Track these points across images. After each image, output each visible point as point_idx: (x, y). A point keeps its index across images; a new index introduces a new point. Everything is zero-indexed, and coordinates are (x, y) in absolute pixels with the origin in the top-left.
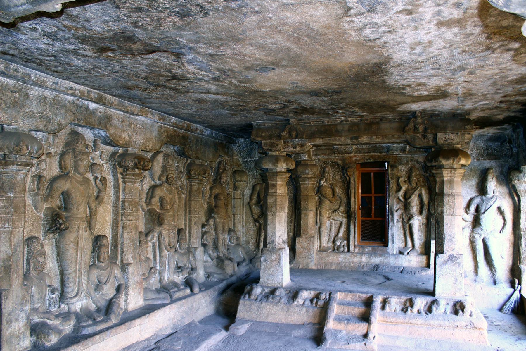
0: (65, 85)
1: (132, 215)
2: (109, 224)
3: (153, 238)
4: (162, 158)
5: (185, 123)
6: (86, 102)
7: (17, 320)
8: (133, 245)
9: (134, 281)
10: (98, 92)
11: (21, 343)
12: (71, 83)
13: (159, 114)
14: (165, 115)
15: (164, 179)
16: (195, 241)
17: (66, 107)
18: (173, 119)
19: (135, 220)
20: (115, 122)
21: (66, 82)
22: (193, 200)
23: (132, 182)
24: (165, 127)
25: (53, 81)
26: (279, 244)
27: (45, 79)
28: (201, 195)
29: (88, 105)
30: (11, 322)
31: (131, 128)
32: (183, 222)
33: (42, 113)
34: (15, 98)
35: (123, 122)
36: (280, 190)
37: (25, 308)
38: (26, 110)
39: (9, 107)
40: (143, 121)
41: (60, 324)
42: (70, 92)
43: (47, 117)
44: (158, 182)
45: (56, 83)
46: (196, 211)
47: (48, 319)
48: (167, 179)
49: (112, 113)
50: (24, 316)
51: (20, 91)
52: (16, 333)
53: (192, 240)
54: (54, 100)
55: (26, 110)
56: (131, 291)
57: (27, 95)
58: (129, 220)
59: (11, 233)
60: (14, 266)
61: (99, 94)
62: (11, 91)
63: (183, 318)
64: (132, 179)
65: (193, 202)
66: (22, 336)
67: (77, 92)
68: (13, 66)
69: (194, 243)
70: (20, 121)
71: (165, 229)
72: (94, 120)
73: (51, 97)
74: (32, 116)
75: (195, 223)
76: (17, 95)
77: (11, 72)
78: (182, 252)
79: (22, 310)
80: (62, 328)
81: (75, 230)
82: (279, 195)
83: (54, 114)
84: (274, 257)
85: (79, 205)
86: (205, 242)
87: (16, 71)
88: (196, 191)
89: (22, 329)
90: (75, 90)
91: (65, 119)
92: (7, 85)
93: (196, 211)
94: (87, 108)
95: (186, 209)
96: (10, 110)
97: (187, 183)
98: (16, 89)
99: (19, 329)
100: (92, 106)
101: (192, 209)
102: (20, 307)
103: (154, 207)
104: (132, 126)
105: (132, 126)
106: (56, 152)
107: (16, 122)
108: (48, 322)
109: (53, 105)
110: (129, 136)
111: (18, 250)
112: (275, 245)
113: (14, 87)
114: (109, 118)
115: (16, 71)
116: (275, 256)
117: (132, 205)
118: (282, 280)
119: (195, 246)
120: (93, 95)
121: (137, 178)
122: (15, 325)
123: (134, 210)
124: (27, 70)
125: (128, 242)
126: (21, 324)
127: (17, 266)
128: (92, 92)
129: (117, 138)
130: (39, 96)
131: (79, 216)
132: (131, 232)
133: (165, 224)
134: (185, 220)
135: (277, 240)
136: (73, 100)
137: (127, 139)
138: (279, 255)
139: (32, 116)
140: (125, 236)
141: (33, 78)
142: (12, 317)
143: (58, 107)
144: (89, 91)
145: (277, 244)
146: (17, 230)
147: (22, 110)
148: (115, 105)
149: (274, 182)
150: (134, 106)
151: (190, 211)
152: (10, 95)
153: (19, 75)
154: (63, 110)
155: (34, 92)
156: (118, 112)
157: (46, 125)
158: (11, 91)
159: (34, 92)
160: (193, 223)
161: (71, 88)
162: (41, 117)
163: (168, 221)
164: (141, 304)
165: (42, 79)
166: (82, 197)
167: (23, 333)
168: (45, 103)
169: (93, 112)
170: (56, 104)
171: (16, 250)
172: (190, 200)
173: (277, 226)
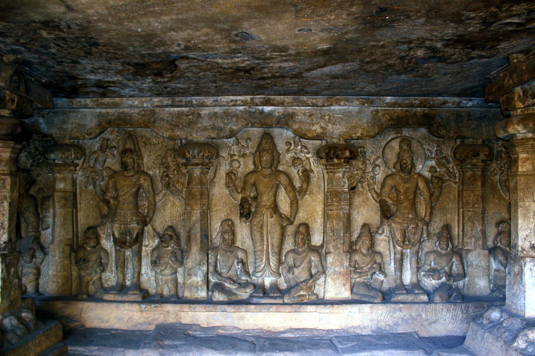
0: (225, 100)
1: (333, 205)
2: (320, 213)
3: (383, 232)
4: (398, 144)
5: (415, 99)
6: (260, 108)
7: (195, 275)
8: (334, 234)
9: (335, 271)
10: (263, 96)
11: (199, 293)
12: (231, 97)
13: (361, 98)
14: (370, 97)
15: (398, 167)
16: (468, 241)
17: (237, 116)
18: (388, 99)
19: (337, 210)
20: (299, 117)
21: (226, 97)
22: (466, 190)
23: (331, 172)
24: (384, 110)
25: (212, 100)
26: (523, 250)
27: (205, 101)
28: (479, 184)
29: (263, 109)
30: (191, 275)
31: (325, 119)
32: (456, 218)
33: (214, 125)
34: (189, 119)
35: (310, 116)
36: (522, 166)
37: (203, 269)
38: (199, 125)
39: (185, 126)
40: (343, 110)
41: (236, 289)
42: (231, 104)
43: (219, 127)
44: (394, 170)
45: (217, 100)
46: (469, 204)
47: (225, 281)
48: (401, 166)
49: (294, 111)
50: (202, 274)
51: (193, 114)
52: (195, 284)
53: (465, 240)
54: (224, 113)
55: (199, 125)
56: (329, 280)
57: (199, 115)
58: (330, 210)
59: (191, 213)
60: (193, 237)
61: (264, 98)
62: (187, 115)
63: (397, 324)
64: (331, 169)
65: (464, 193)
66: (199, 288)
67: (238, 102)
68: (177, 99)
69: (467, 243)
70: (194, 135)
71: (396, 222)
72: (271, 121)
73: (222, 111)
74: (205, 129)
75: (469, 219)
76: (191, 117)
77: (177, 104)
78: (443, 252)
79: (200, 269)
80: (238, 293)
81: (258, 215)
82: (522, 175)
83: (225, 124)
84: (517, 269)
85: (262, 195)
86: (499, 244)
87: (181, 101)
88: (469, 178)
89: (200, 283)
90: (237, 101)
91: (236, 126)
92: (183, 112)
93: (469, 204)
94: (262, 112)
95: (459, 202)
96: (185, 129)
97: (458, 169)
98: (190, 113)
99: (198, 282)
100: (267, 109)
101: (465, 200)
102: (198, 267)
103: (384, 198)
104: (327, 117)
105: (327, 117)
106: (251, 152)
107: (191, 135)
108: (226, 284)
109: (224, 117)
110: (322, 128)
111: (196, 225)
112: (518, 251)
113: (188, 112)
114: (291, 116)
115: (181, 101)
116: (517, 267)
117: (332, 195)
118: (524, 307)
119: (469, 248)
120: (257, 101)
121: (335, 167)
122: (194, 278)
123: (334, 199)
124: (189, 99)
125: (330, 231)
126: (199, 279)
127: (196, 237)
128: (256, 98)
129: (304, 132)
130: (210, 113)
131: (262, 204)
132: (332, 222)
133: (397, 217)
134: (459, 215)
135: (520, 243)
136: (245, 109)
137: (319, 130)
138: (521, 267)
139: (205, 129)
140: (328, 226)
141: (194, 102)
142: (192, 272)
143: (229, 118)
144: (251, 99)
145: (520, 249)
146: (195, 211)
147: (195, 126)
148: (288, 103)
149: (515, 156)
150: (316, 99)
151: (462, 203)
152: (185, 118)
153: (183, 103)
154: (234, 119)
155: (205, 112)
156: (302, 108)
157: (217, 134)
158: (187, 115)
159: (205, 112)
160: (466, 219)
161: (232, 101)
162: (212, 129)
163: (402, 213)
164: (347, 296)
165: (202, 101)
166: (266, 187)
167: (201, 286)
168: (216, 117)
169: (270, 114)
170: (227, 116)
171: (195, 226)
172: (462, 191)
173: (520, 221)
